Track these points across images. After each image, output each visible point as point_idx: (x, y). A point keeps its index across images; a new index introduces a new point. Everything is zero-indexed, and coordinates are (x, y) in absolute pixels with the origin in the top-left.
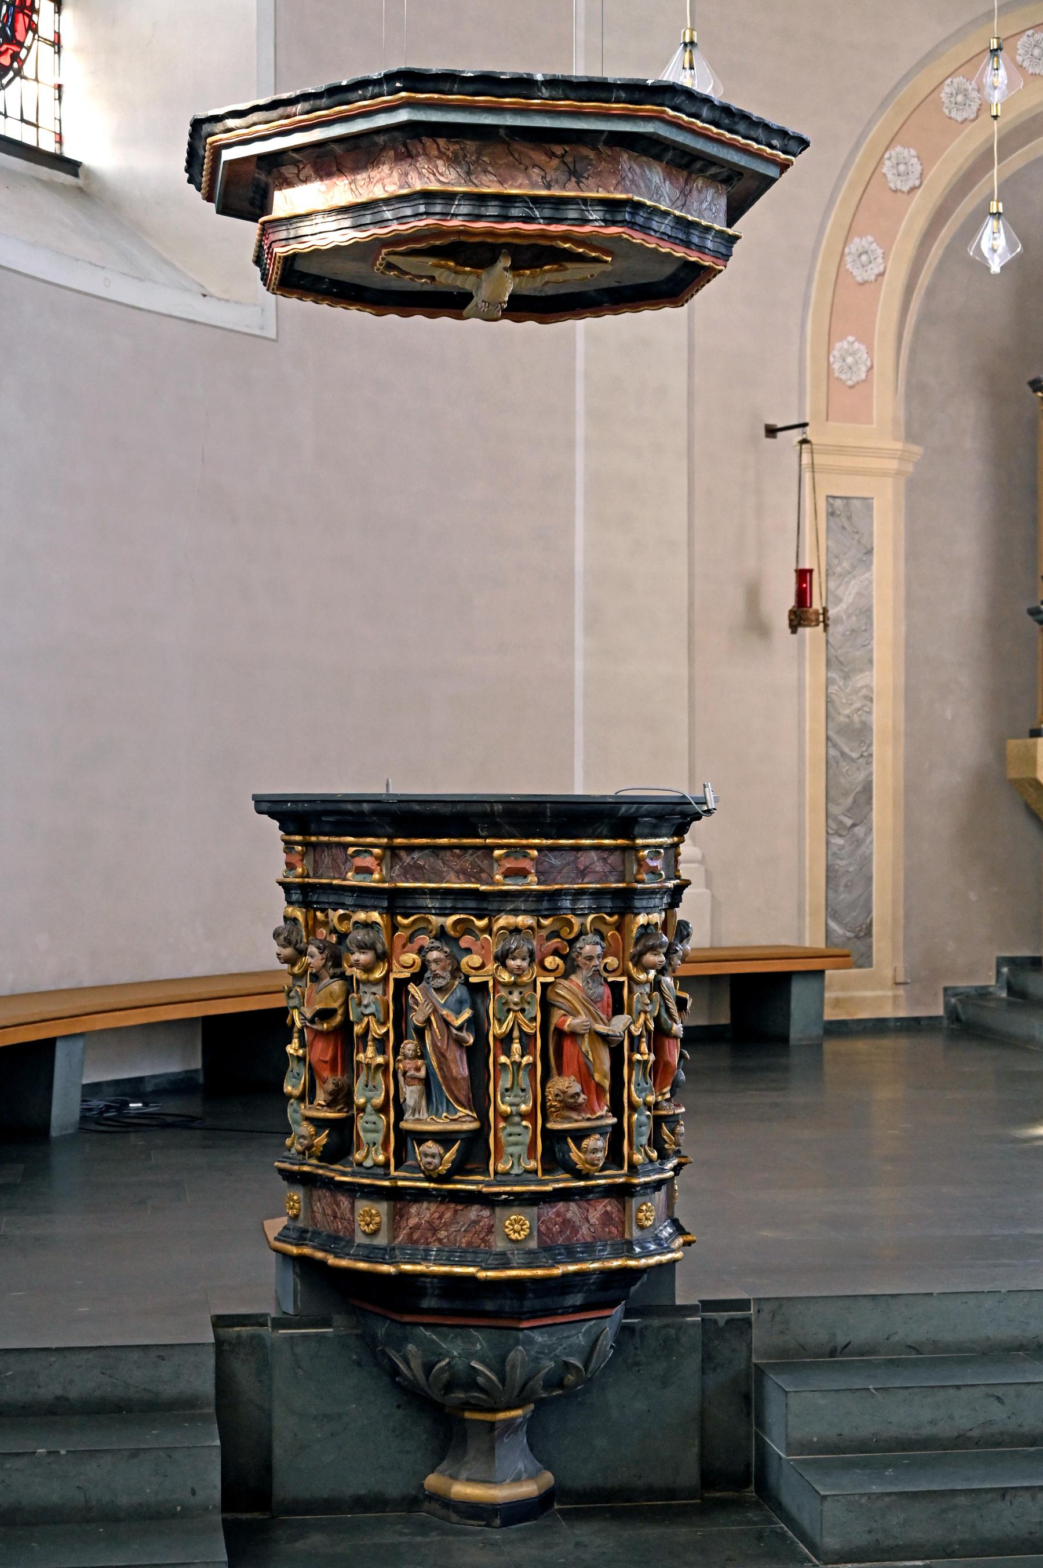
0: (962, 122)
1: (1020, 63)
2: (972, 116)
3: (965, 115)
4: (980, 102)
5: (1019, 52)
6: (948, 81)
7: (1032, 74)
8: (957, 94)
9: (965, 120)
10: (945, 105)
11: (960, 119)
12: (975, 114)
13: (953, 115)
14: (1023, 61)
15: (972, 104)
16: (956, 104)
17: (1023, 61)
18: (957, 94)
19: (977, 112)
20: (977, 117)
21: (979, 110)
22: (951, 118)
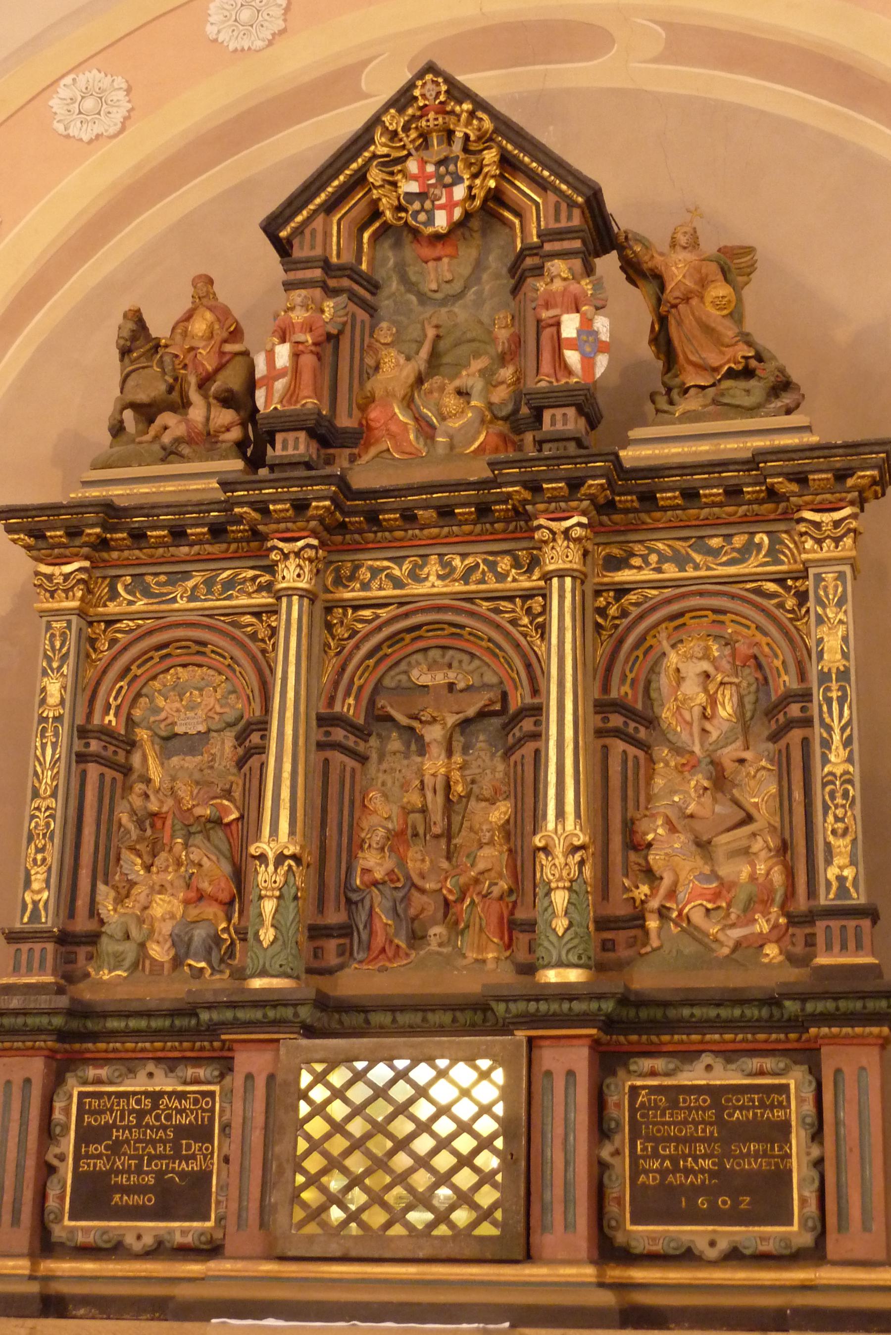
0: (91, 142)
1: (212, 36)
2: (112, 130)
3: (98, 129)
4: (129, 106)
5: (211, 19)
6: (68, 80)
7: (236, 50)
8: (83, 98)
9: (98, 136)
10: (58, 118)
11: (86, 138)
12: (119, 125)
13: (73, 131)
14: (219, 32)
15: (114, 110)
16: (80, 113)
17: (219, 32)
18: (83, 98)
19: (123, 123)
20: (123, 129)
21: (126, 118)
22: (68, 136)
